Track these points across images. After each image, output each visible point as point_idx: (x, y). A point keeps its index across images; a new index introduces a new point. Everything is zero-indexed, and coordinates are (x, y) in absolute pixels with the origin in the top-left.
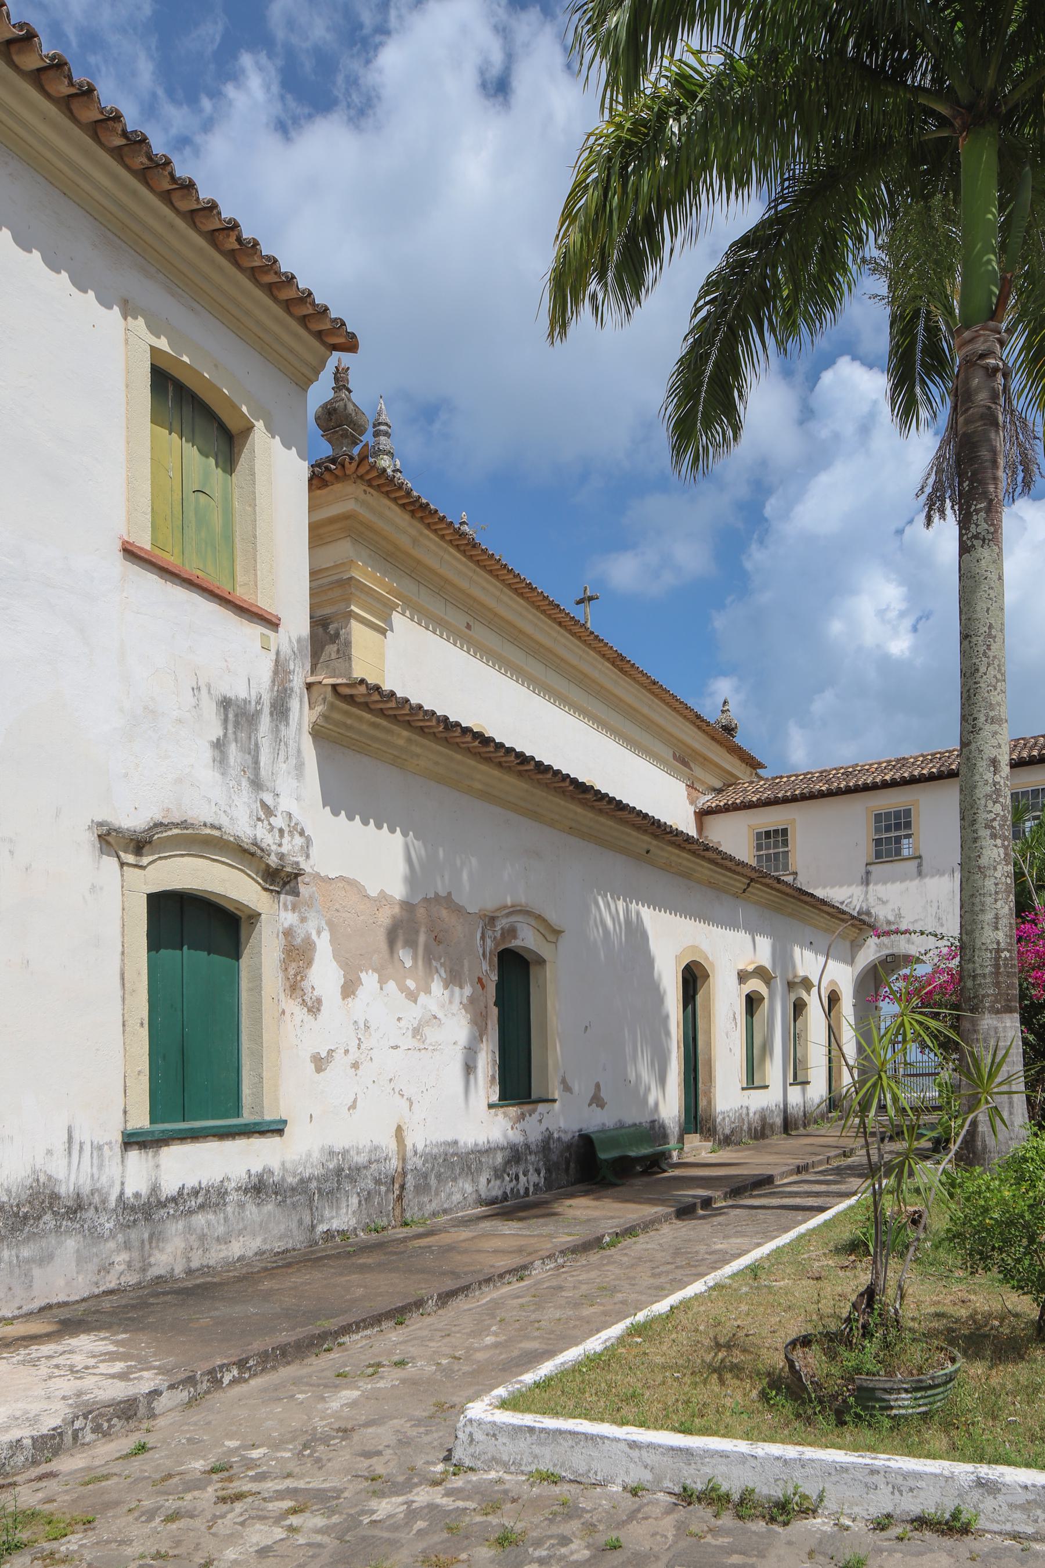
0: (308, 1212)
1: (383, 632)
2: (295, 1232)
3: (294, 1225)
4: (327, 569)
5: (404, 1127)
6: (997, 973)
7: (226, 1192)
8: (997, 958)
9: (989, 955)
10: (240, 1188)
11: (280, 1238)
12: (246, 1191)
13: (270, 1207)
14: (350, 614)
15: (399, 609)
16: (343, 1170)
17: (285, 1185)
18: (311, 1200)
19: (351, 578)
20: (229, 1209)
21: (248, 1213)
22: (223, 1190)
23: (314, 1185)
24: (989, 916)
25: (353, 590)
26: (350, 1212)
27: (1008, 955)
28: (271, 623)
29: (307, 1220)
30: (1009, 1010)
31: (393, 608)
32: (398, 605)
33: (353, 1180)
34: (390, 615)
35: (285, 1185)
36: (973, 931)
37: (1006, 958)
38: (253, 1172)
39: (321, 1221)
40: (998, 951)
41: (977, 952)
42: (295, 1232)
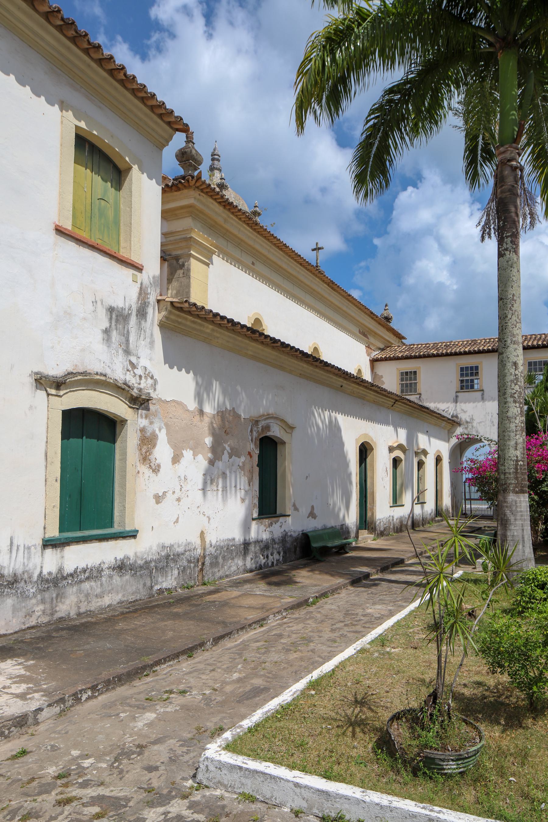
0: (149, 579)
1: (208, 265)
2: (141, 590)
3: (141, 587)
4: (179, 232)
5: (205, 532)
6: (516, 473)
7: (102, 570)
8: (517, 465)
9: (512, 463)
10: (110, 567)
11: (133, 594)
12: (114, 569)
13: (127, 577)
14: (190, 255)
15: (217, 254)
16: (170, 556)
17: (137, 565)
18: (151, 573)
19: (191, 237)
20: (104, 579)
21: (114, 581)
22: (100, 569)
23: (153, 564)
24: (512, 443)
25: (192, 243)
26: (173, 578)
27: (522, 463)
28: (139, 268)
29: (148, 583)
30: (522, 492)
31: (214, 253)
32: (216, 252)
33: (175, 561)
34: (212, 257)
35: (137, 565)
36: (504, 450)
37: (521, 465)
38: (118, 558)
39: (156, 584)
40: (517, 461)
41: (506, 461)
42: (141, 590)
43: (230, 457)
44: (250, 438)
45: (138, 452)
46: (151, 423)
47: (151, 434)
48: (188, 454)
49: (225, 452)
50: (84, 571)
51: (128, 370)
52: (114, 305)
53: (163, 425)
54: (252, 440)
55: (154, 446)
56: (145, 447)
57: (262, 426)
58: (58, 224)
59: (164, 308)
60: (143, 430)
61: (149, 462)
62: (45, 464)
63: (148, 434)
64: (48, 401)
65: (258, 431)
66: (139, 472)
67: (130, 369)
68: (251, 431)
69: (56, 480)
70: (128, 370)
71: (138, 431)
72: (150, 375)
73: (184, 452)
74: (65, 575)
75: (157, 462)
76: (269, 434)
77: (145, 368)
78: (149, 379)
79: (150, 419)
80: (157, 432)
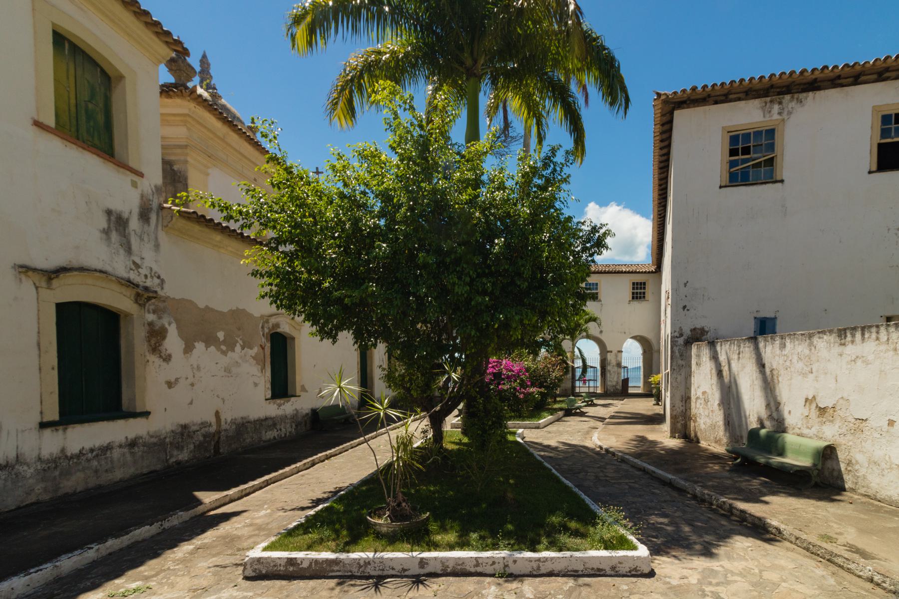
5: (220, 411)
43: (243, 349)
44: (261, 333)
45: (146, 344)
46: (160, 318)
47: (160, 328)
48: (200, 346)
49: (238, 345)
50: (92, 450)
51: (131, 269)
52: (112, 207)
53: (172, 320)
54: (263, 335)
55: (164, 338)
56: (154, 339)
57: (273, 324)
58: (36, 118)
59: (169, 216)
60: (151, 324)
61: (159, 352)
62: (37, 352)
63: (157, 327)
64: (38, 293)
65: (269, 328)
66: (148, 361)
67: (134, 268)
68: (263, 327)
69: (53, 369)
70: (131, 269)
71: (146, 325)
72: (157, 275)
73: (196, 344)
74: (69, 454)
75: (167, 352)
76: (279, 330)
77: (151, 269)
78: (155, 279)
79: (158, 314)
80: (167, 326)
